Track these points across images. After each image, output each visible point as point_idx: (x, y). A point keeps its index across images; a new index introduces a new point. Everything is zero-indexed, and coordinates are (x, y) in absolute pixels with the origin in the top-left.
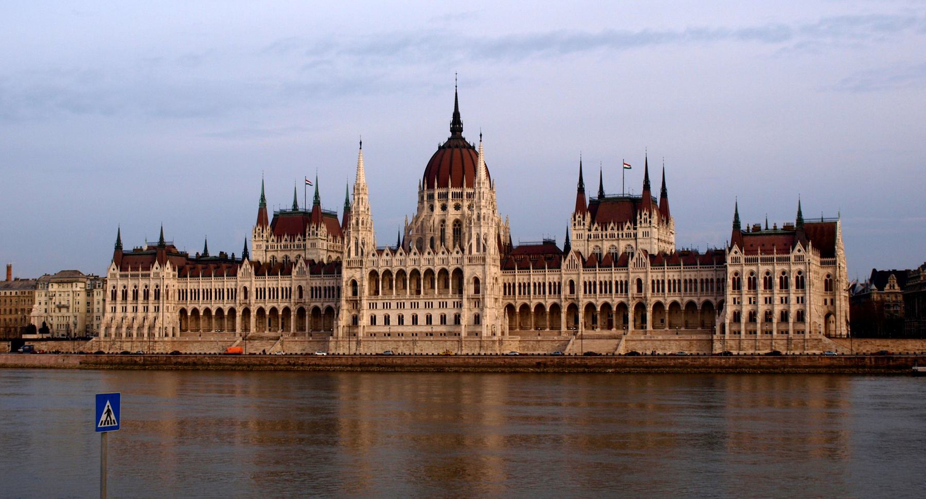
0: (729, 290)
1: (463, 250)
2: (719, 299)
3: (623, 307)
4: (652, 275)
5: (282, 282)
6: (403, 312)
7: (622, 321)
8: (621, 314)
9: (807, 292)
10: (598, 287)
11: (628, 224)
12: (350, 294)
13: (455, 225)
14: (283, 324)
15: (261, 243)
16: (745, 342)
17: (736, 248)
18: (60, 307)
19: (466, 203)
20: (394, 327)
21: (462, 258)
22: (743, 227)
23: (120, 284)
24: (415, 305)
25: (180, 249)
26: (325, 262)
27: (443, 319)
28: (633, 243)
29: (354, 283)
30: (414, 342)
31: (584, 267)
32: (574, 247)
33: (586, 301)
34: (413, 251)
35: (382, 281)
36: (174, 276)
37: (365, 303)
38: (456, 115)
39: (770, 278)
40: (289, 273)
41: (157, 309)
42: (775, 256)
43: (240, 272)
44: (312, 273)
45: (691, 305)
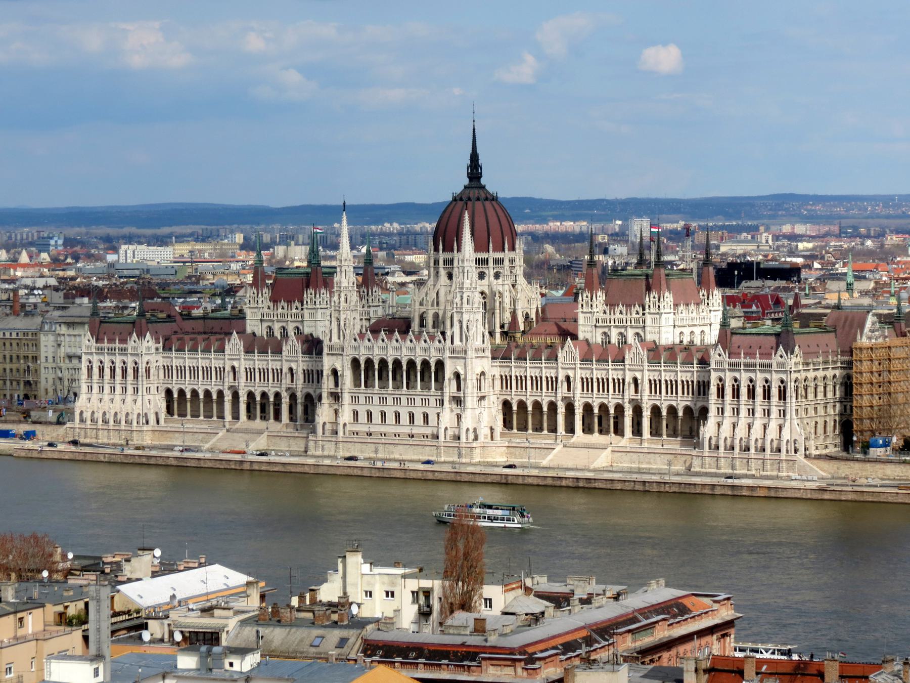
1: (445, 340)
5: (271, 362)
6: (385, 409)
9: (788, 404)
10: (595, 385)
16: (723, 460)
18: (70, 357)
20: (377, 428)
23: (95, 359)
29: (335, 372)
31: (582, 360)
35: (368, 372)
36: (157, 349)
37: (346, 398)
38: (474, 157)
41: (136, 390)
42: (758, 361)
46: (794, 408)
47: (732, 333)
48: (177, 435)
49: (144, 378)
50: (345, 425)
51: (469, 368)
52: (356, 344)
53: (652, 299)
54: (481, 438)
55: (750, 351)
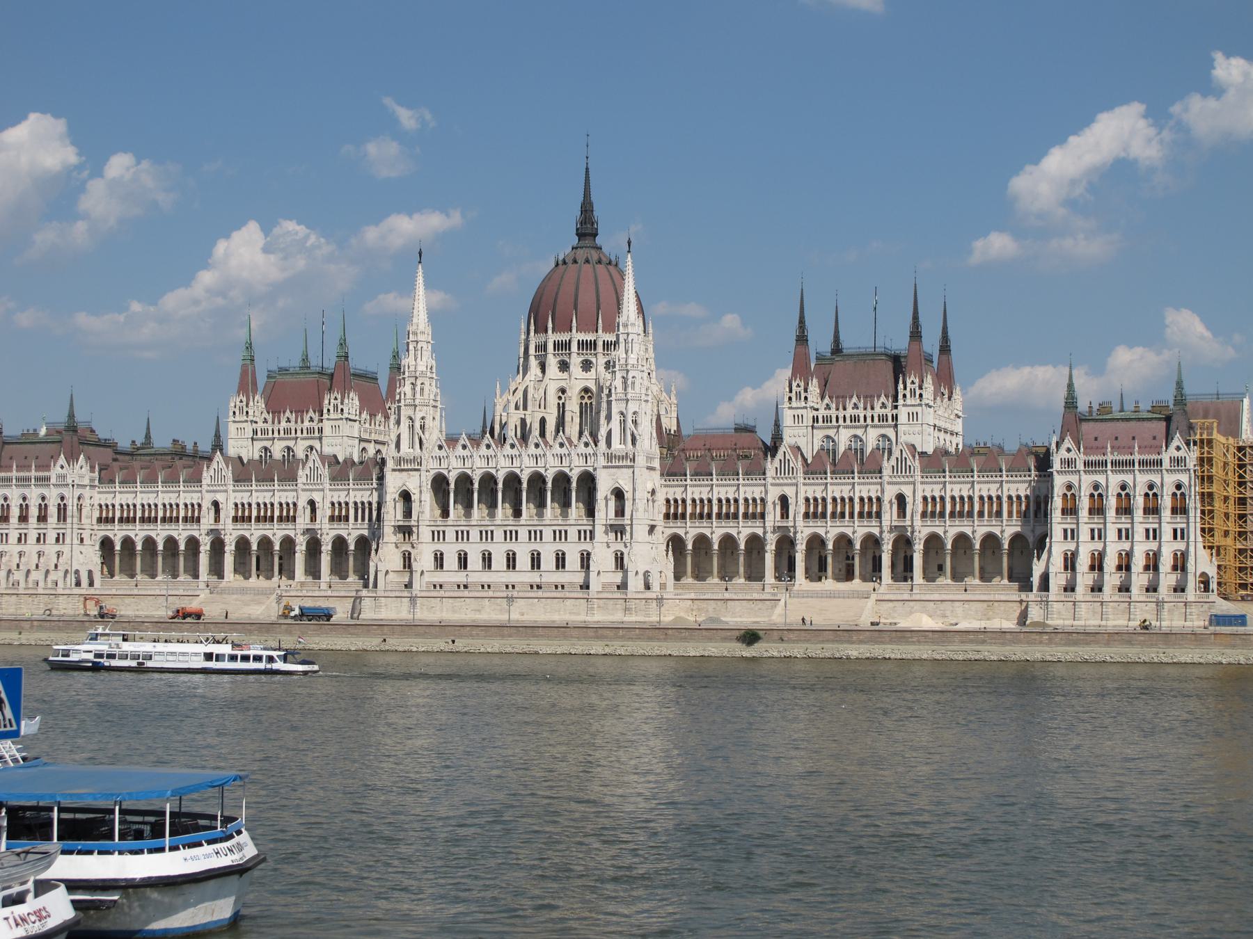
0: (1057, 516)
2: (1039, 530)
3: (872, 542)
4: (920, 489)
5: (280, 495)
6: (490, 547)
7: (870, 567)
8: (870, 557)
9: (1192, 519)
11: (883, 399)
12: (400, 516)
13: (583, 398)
14: (280, 565)
15: (245, 425)
17: (1068, 442)
19: (602, 360)
21: (595, 454)
22: (1082, 406)
24: (511, 535)
25: (102, 434)
26: (356, 460)
27: (561, 561)
28: (890, 433)
29: (406, 496)
30: (510, 599)
31: (805, 473)
32: (789, 438)
33: (808, 532)
34: (509, 441)
36: (92, 480)
37: (425, 533)
38: (587, 209)
39: (1127, 495)
40: (294, 478)
43: (206, 476)
44: (333, 479)
45: (991, 541)
46: (1199, 526)
47: (1081, 420)
48: (127, 600)
49: (75, 520)
50: (422, 573)
51: (638, 482)
52: (443, 453)
53: (909, 385)
54: (655, 586)
55: (1117, 443)
